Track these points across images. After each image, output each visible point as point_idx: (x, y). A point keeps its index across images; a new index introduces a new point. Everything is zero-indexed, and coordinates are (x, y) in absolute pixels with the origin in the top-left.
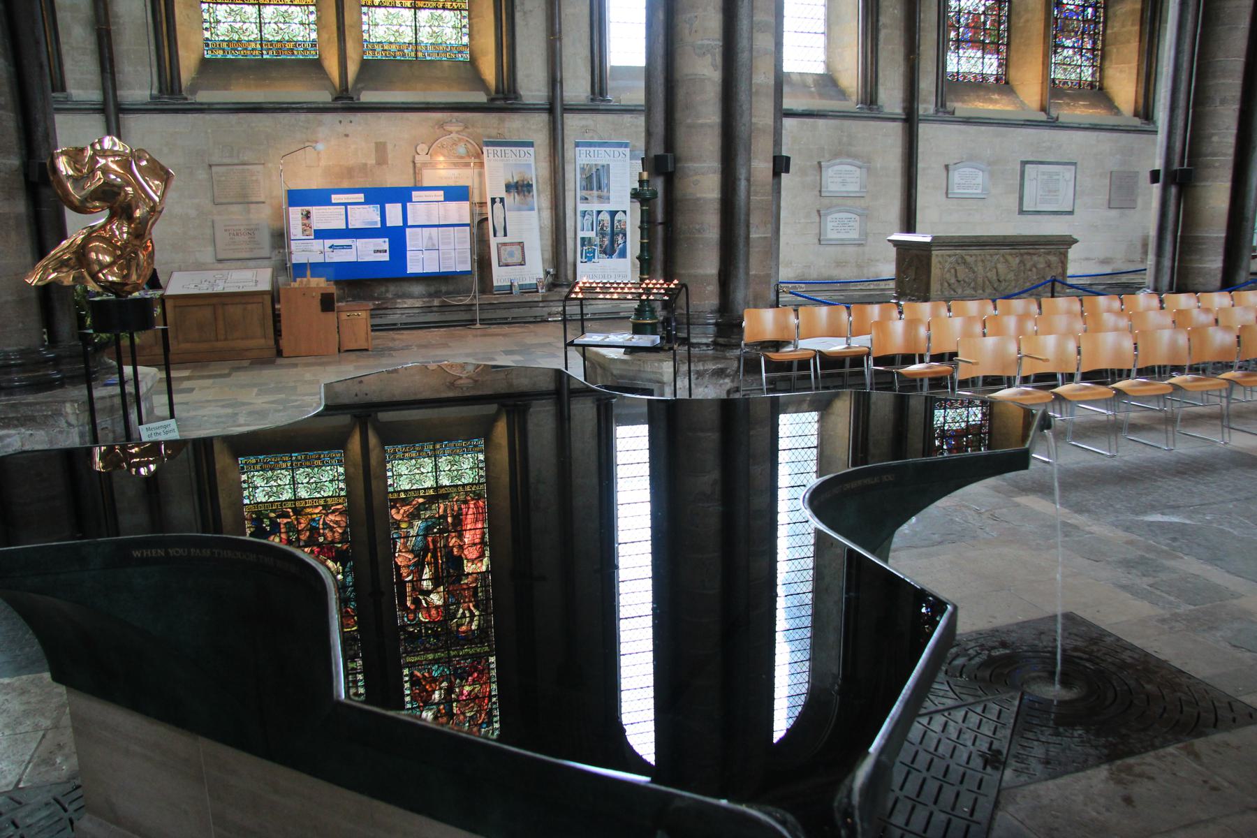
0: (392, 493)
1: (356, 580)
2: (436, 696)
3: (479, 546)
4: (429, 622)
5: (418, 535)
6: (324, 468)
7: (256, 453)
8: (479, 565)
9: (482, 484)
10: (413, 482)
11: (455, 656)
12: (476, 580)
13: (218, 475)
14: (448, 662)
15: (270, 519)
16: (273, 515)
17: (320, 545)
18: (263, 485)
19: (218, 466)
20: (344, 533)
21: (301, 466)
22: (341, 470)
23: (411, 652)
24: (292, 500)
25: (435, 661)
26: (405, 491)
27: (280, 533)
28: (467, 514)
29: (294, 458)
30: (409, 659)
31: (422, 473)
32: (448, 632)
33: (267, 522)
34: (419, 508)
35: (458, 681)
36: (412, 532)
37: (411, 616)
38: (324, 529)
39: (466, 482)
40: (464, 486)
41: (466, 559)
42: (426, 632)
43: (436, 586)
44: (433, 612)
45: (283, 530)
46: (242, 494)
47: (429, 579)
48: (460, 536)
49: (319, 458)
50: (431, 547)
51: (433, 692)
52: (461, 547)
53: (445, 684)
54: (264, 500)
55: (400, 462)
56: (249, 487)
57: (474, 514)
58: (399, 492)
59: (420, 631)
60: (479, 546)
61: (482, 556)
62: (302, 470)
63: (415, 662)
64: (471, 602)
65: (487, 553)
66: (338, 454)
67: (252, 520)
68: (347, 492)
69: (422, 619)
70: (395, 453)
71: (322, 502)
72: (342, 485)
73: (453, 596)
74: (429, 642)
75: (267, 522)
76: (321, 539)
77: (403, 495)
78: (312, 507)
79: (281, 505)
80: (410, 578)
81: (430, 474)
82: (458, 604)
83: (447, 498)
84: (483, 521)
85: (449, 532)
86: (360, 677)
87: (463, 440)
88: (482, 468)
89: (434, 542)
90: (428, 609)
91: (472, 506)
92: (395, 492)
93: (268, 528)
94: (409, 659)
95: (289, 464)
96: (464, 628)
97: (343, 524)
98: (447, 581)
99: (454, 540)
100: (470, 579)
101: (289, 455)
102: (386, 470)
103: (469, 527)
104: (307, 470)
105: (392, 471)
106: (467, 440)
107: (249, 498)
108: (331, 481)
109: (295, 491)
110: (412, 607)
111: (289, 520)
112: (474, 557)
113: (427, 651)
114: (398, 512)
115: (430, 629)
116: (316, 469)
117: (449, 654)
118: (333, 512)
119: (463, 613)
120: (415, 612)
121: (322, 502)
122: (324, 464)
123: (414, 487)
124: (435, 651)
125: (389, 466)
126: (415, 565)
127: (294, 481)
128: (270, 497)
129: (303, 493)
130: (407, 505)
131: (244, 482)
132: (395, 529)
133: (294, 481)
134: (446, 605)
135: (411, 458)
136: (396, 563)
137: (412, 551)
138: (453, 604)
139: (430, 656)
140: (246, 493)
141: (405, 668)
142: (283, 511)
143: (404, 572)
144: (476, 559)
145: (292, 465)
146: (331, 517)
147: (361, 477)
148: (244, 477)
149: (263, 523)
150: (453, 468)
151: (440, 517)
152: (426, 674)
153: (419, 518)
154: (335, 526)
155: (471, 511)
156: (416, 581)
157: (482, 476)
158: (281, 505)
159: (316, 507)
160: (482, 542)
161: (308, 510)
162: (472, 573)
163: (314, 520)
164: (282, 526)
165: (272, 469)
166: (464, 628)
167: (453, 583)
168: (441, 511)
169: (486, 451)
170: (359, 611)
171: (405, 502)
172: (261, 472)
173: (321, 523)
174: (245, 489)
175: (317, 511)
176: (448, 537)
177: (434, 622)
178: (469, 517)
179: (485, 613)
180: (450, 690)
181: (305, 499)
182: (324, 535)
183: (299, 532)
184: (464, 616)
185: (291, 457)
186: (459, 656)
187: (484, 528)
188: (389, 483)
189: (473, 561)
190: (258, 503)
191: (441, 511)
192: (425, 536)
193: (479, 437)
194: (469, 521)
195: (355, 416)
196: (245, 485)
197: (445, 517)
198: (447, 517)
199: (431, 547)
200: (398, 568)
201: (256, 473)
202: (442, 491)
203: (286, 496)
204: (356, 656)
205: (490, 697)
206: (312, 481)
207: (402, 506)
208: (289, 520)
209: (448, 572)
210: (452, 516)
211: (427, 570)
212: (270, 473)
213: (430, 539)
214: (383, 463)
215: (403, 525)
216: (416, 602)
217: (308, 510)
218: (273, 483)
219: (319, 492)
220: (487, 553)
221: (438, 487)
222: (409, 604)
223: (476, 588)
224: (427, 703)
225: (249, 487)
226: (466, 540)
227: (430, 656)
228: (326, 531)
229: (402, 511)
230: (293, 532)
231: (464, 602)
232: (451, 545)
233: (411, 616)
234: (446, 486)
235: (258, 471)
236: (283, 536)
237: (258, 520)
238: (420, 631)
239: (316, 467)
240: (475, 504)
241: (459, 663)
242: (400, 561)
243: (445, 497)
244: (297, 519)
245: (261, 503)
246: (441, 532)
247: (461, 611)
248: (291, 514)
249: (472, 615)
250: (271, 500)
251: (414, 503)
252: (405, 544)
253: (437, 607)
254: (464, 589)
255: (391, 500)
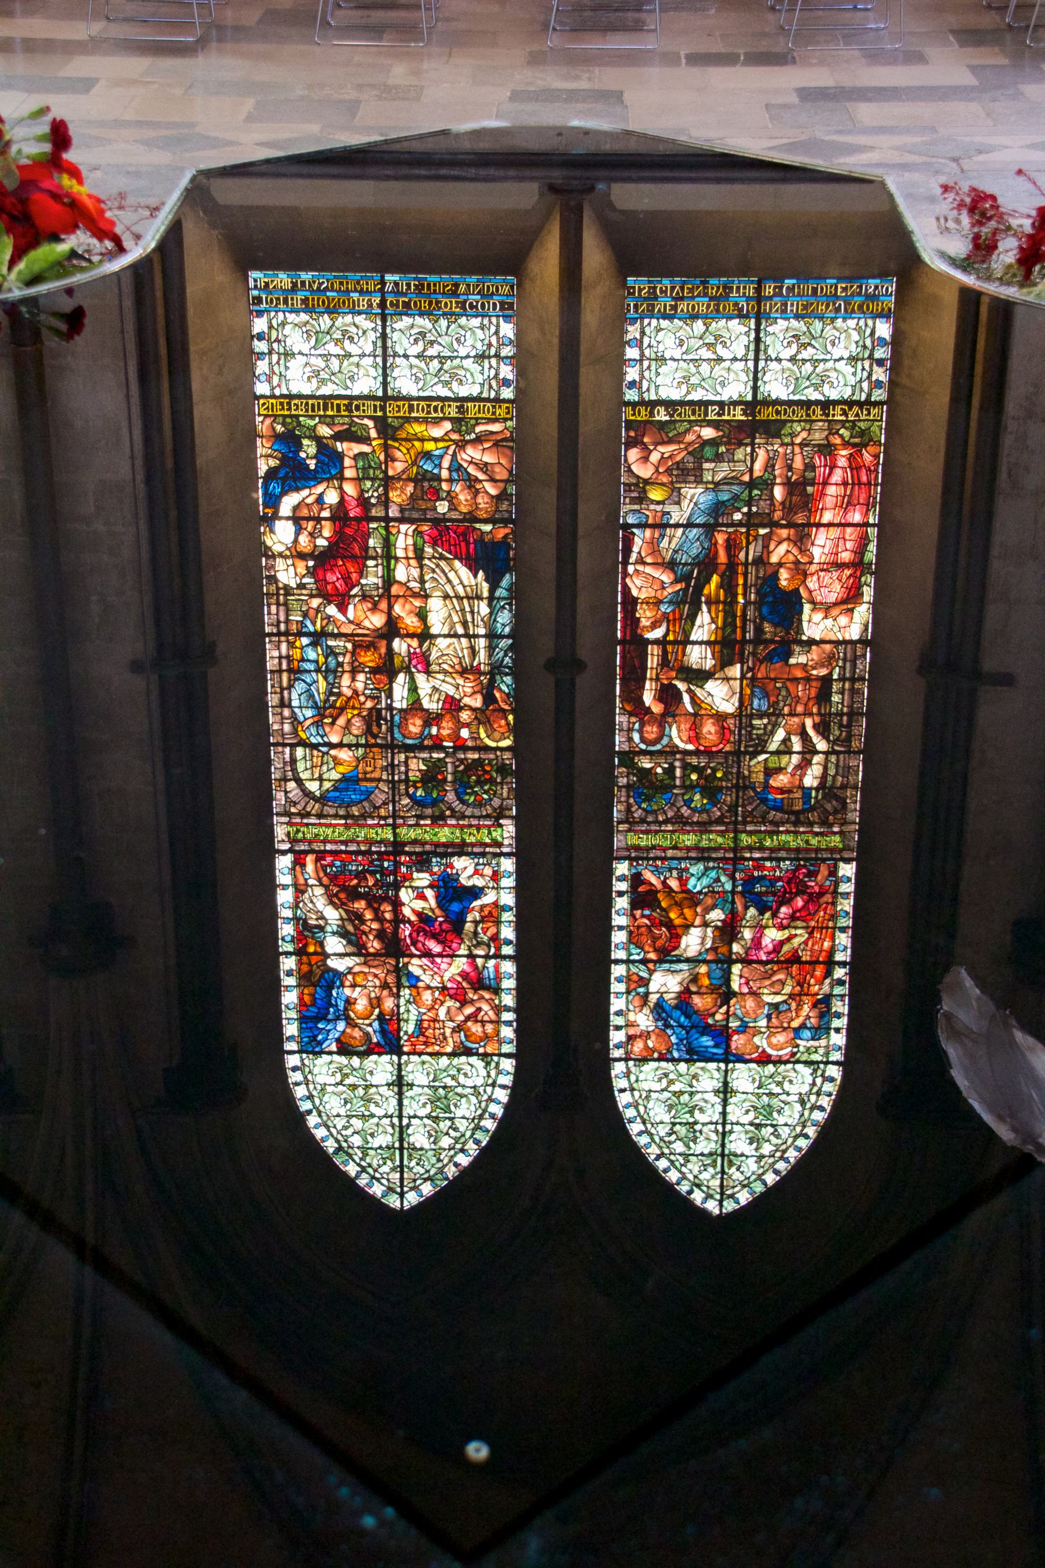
0: (634, 405)
1: (519, 619)
2: (692, 942)
3: (848, 572)
4: (697, 753)
5: (689, 525)
6: (463, 321)
7: (293, 265)
8: (843, 620)
9: (876, 404)
10: (694, 380)
11: (750, 848)
12: (831, 658)
13: (191, 312)
14: (734, 859)
15: (318, 440)
16: (325, 431)
17: (438, 522)
18: (306, 351)
19: (193, 290)
20: (499, 498)
21: (407, 309)
22: (508, 330)
23: (643, 821)
24: (374, 398)
25: (702, 855)
26: (670, 405)
27: (342, 478)
28: (826, 483)
29: (389, 287)
30: (632, 839)
31: (720, 360)
32: (742, 785)
33: (309, 448)
34: (700, 452)
35: (752, 911)
36: (677, 515)
37: (651, 731)
38: (450, 480)
39: (834, 395)
40: (826, 405)
41: (812, 602)
42: (685, 776)
43: (724, 662)
44: (709, 728)
45: (349, 473)
46: (253, 367)
47: (708, 643)
48: (802, 539)
49: (454, 293)
50: (722, 557)
51: (687, 927)
52: (800, 571)
53: (717, 915)
54: (306, 391)
55: (664, 323)
56: (270, 352)
57: (845, 484)
58: (653, 404)
59: (670, 771)
60: (848, 572)
61: (851, 598)
62: (407, 321)
63: (648, 849)
64: (811, 714)
65: (868, 593)
66: (502, 284)
67: (277, 437)
68: (518, 390)
69: (677, 741)
70: (653, 296)
71: (453, 412)
72: (507, 372)
73: (766, 695)
74: (688, 803)
75: (309, 448)
76: (442, 507)
77: (661, 415)
78: (425, 421)
79: (348, 408)
80: (658, 633)
81: (740, 365)
82: (774, 715)
83: (778, 435)
84: (868, 507)
85: (774, 525)
86: (508, 865)
87: (840, 279)
88: (880, 362)
89: (731, 546)
90: (696, 719)
91: (842, 462)
92: (642, 403)
93: (312, 464)
94: (632, 839)
95: (376, 300)
96: (781, 780)
97: (501, 474)
98: (754, 654)
99: (783, 548)
100: (815, 653)
101: (377, 276)
102: (624, 344)
103: (827, 517)
104: (419, 321)
105: (640, 343)
106: (850, 279)
107: (269, 380)
108: (481, 357)
109: (385, 375)
110: (657, 709)
111: (366, 449)
112: (832, 598)
113: (681, 822)
114: (645, 459)
115: (695, 769)
116: (443, 323)
117: (736, 839)
118: (479, 440)
119: (786, 741)
120: (662, 722)
121: (453, 412)
122: (466, 309)
123: (695, 396)
124: (703, 827)
125: (633, 331)
126: (677, 601)
127: (384, 347)
128: (323, 382)
129: (404, 384)
130: (670, 441)
131: (260, 337)
132: (633, 501)
133: (384, 347)
134: (743, 713)
135: (694, 317)
136: (626, 590)
137: (671, 565)
138: (761, 717)
139: (689, 840)
140: (262, 367)
141: (619, 859)
142: (352, 424)
143: (645, 615)
144: (836, 604)
145: (382, 305)
146: (472, 452)
147: (553, 358)
148: (260, 325)
149: (300, 447)
150: (805, 354)
151: (752, 484)
152: (674, 884)
153: (699, 481)
154: (481, 476)
155: (837, 476)
156: (675, 642)
157: (878, 384)
158: (348, 408)
159: (437, 421)
160: (858, 565)
161: (418, 428)
162: (823, 642)
163: (427, 455)
164: (347, 462)
165: (332, 311)
166: (781, 780)
167: (769, 658)
168: (758, 466)
169: (898, 316)
170: (518, 695)
171: (664, 433)
172: (304, 317)
173: (446, 463)
174: (260, 356)
175: (437, 432)
176: (768, 538)
177: (708, 753)
178: (831, 490)
179: (842, 747)
180: (729, 931)
181: (409, 399)
182: (451, 497)
183: (388, 482)
184: (786, 749)
185: (383, 283)
186: (762, 848)
187: (866, 524)
188: (629, 378)
189: (827, 609)
190: (290, 397)
191: (758, 466)
192: (710, 529)
193: (883, 275)
194: (829, 501)
195: (553, 189)
196: (261, 346)
197: (768, 485)
198: (774, 484)
199: (722, 557)
200: (631, 603)
201: (291, 317)
202: (767, 414)
203: (366, 383)
204: (499, 814)
205: (830, 964)
206: (432, 352)
207: (656, 444)
208: (366, 449)
209: (759, 630)
210: (788, 483)
211: (704, 617)
212: (325, 321)
213: (721, 538)
214: (619, 320)
215: (655, 494)
216: (668, 695)
217: (418, 428)
218: (332, 349)
219: (446, 384)
220: (868, 593)
221: (754, 404)
222: (648, 698)
223: (827, 680)
224: (667, 955)
225: (270, 352)
226: (816, 552)
227: (689, 840)
228: (457, 488)
229: (655, 457)
230: (373, 480)
231: (792, 714)
232: (774, 559)
233: (651, 731)
234: (778, 402)
235: (297, 312)
236: (350, 489)
237: (289, 440)
238: (670, 771)
239: (444, 314)
240: (850, 458)
241: (758, 865)
242: (638, 587)
243: (772, 430)
244: (386, 448)
245: (300, 397)
246: (751, 522)
247: (780, 734)
248: (373, 433)
249: (809, 750)
250: (327, 390)
251: (690, 437)
252: (654, 546)
253: (720, 718)
254: (796, 680)
255: (630, 425)
